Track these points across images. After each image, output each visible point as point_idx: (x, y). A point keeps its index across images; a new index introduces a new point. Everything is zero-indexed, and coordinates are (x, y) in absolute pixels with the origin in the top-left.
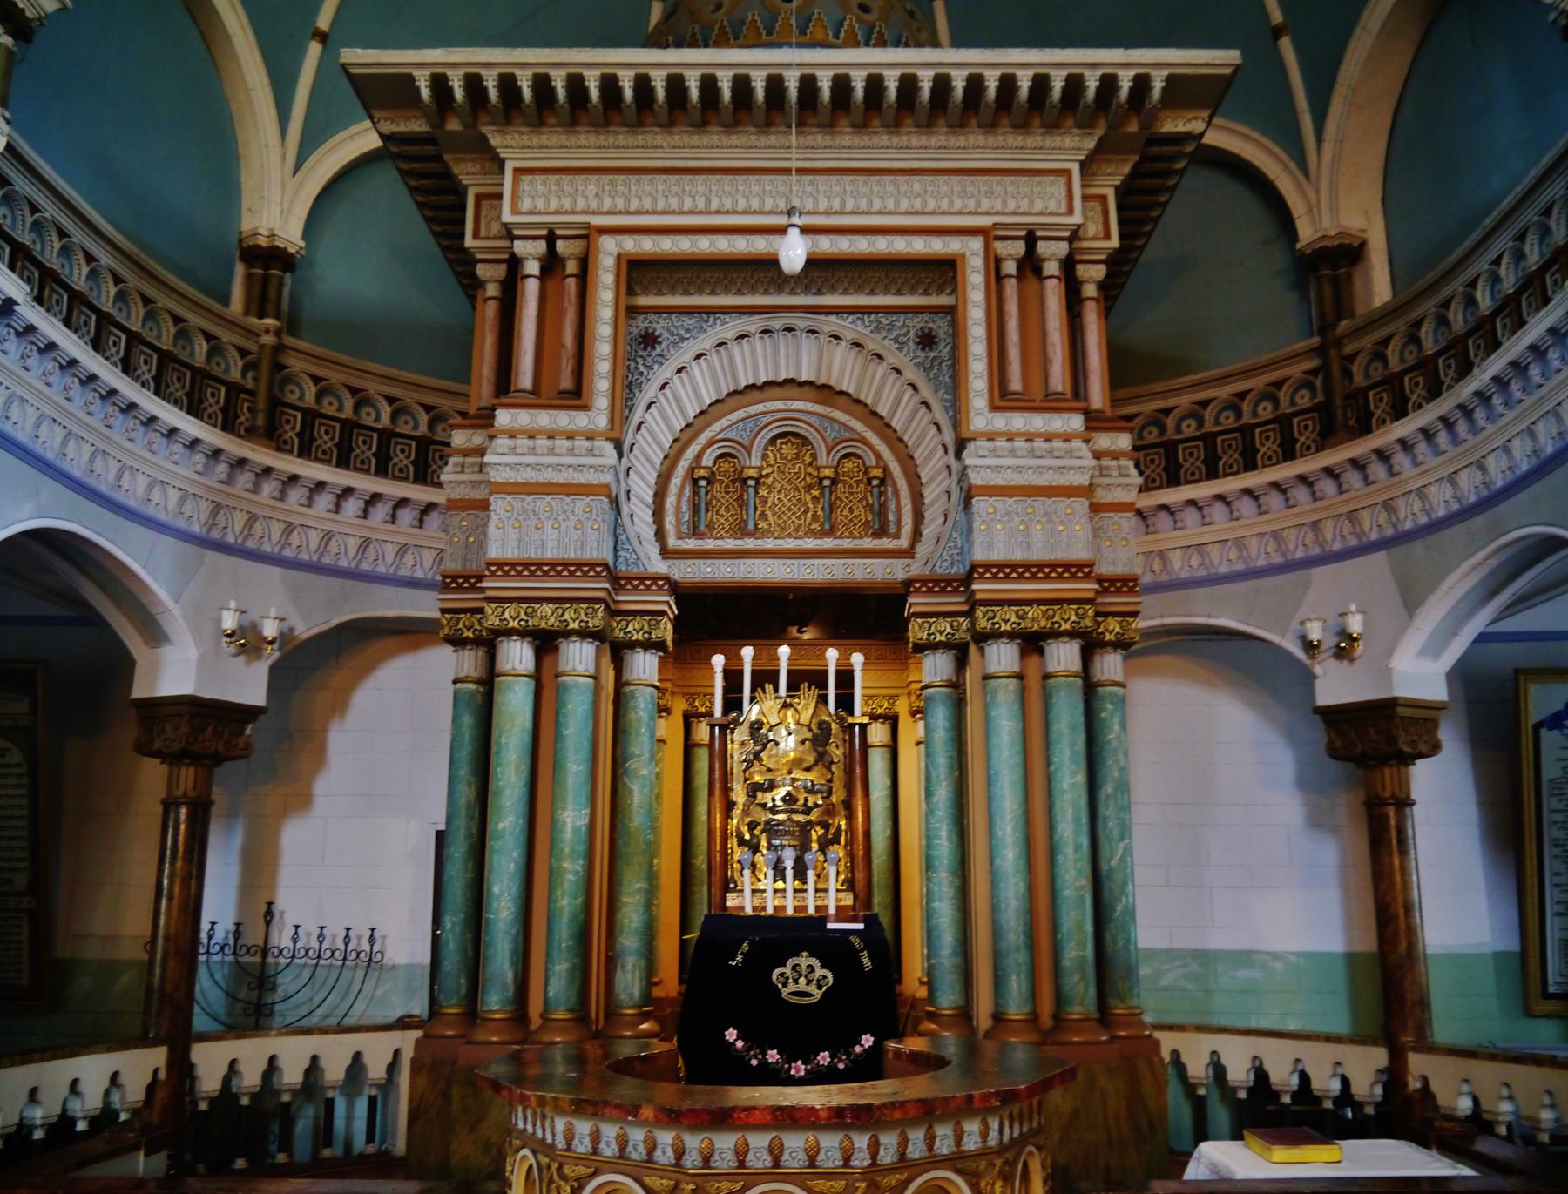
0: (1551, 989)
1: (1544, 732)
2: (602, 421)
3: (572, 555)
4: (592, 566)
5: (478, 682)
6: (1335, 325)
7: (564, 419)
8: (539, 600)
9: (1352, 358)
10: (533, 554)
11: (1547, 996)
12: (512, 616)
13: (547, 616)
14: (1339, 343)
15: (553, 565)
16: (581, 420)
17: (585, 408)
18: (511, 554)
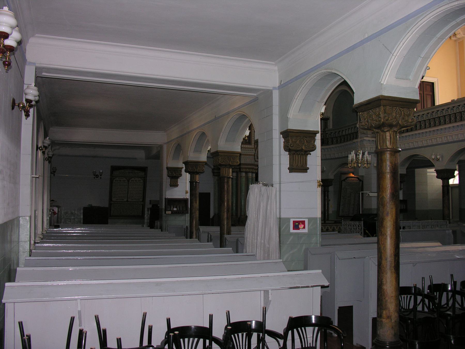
0: (340, 215)
1: (343, 181)
2: (253, 147)
3: (250, 163)
4: (253, 164)
5: (236, 177)
6: (325, 129)
7: (249, 146)
8: (247, 168)
9: (327, 133)
10: (246, 163)
11: (339, 216)
12: (244, 170)
13: (248, 170)
14: (325, 132)
15: (248, 164)
16: (251, 146)
17: (251, 145)
18: (244, 163)
